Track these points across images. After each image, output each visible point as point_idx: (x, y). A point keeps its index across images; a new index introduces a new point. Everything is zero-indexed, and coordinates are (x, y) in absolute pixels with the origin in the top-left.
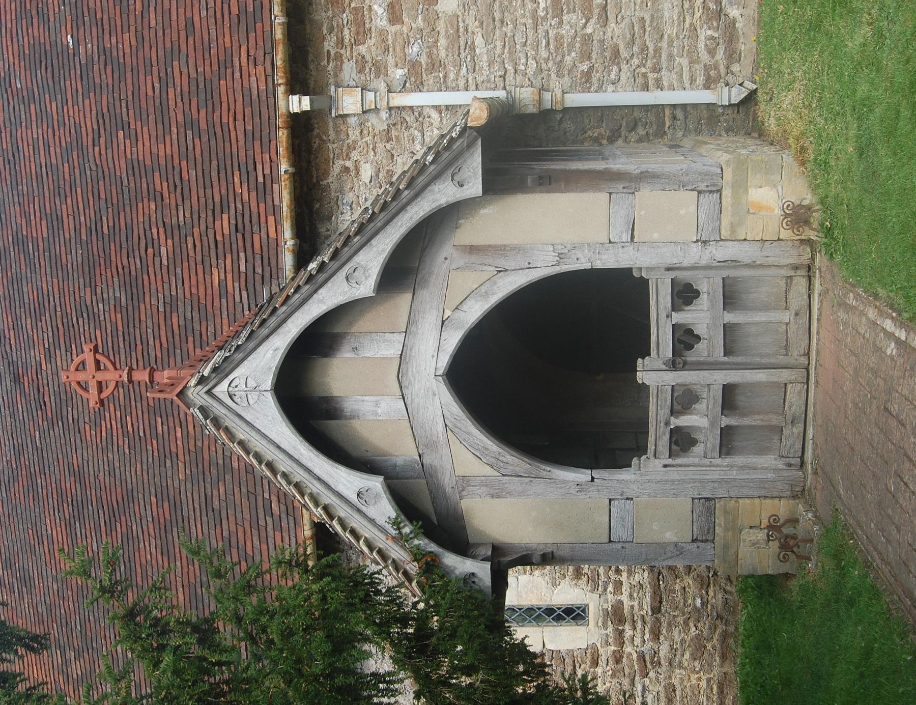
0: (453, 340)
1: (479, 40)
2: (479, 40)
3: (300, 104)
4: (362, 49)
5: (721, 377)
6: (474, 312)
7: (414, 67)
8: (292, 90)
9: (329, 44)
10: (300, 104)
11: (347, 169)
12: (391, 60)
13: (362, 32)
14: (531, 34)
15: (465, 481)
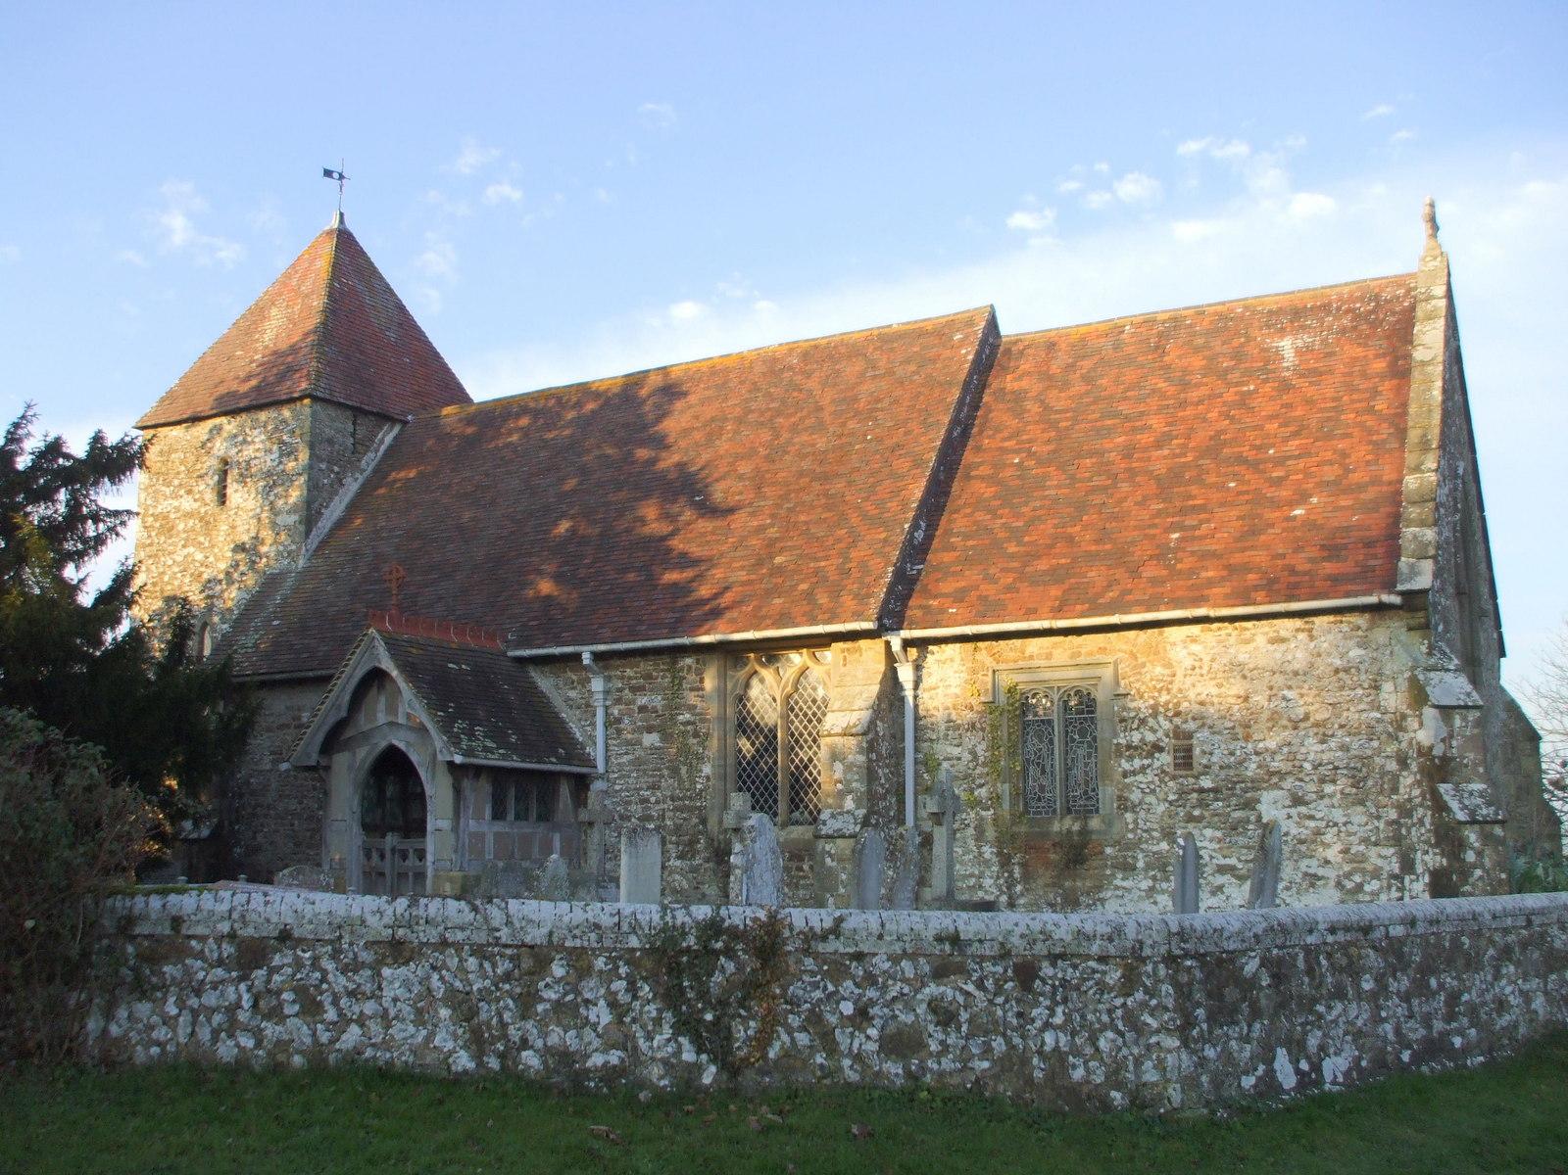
0: (402, 746)
1: (630, 757)
2: (630, 757)
3: (586, 659)
4: (627, 691)
5: (387, 872)
6: (414, 758)
7: (619, 721)
8: (592, 653)
9: (629, 672)
10: (586, 659)
11: (573, 682)
12: (622, 707)
13: (635, 690)
14: (633, 787)
15: (354, 754)
